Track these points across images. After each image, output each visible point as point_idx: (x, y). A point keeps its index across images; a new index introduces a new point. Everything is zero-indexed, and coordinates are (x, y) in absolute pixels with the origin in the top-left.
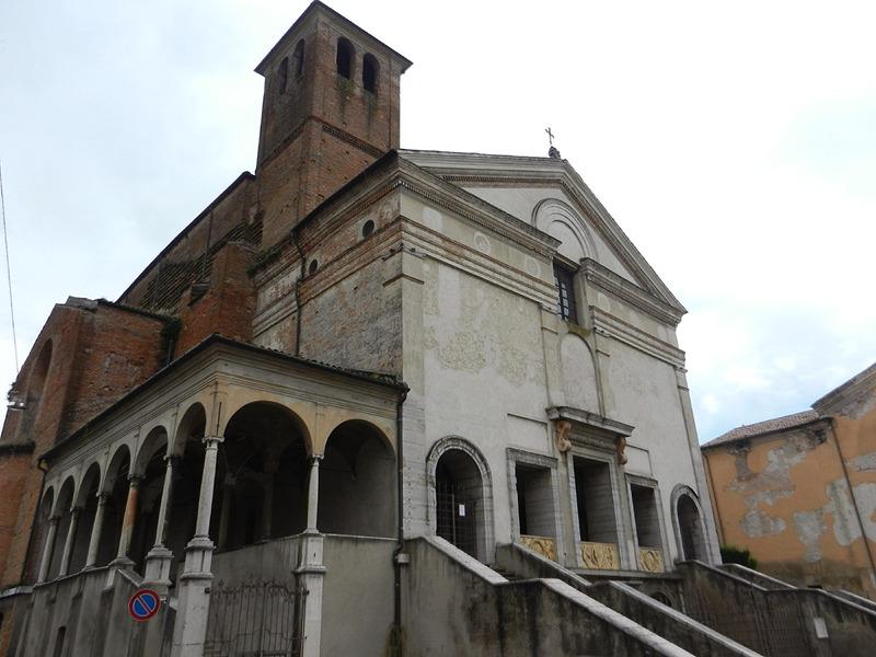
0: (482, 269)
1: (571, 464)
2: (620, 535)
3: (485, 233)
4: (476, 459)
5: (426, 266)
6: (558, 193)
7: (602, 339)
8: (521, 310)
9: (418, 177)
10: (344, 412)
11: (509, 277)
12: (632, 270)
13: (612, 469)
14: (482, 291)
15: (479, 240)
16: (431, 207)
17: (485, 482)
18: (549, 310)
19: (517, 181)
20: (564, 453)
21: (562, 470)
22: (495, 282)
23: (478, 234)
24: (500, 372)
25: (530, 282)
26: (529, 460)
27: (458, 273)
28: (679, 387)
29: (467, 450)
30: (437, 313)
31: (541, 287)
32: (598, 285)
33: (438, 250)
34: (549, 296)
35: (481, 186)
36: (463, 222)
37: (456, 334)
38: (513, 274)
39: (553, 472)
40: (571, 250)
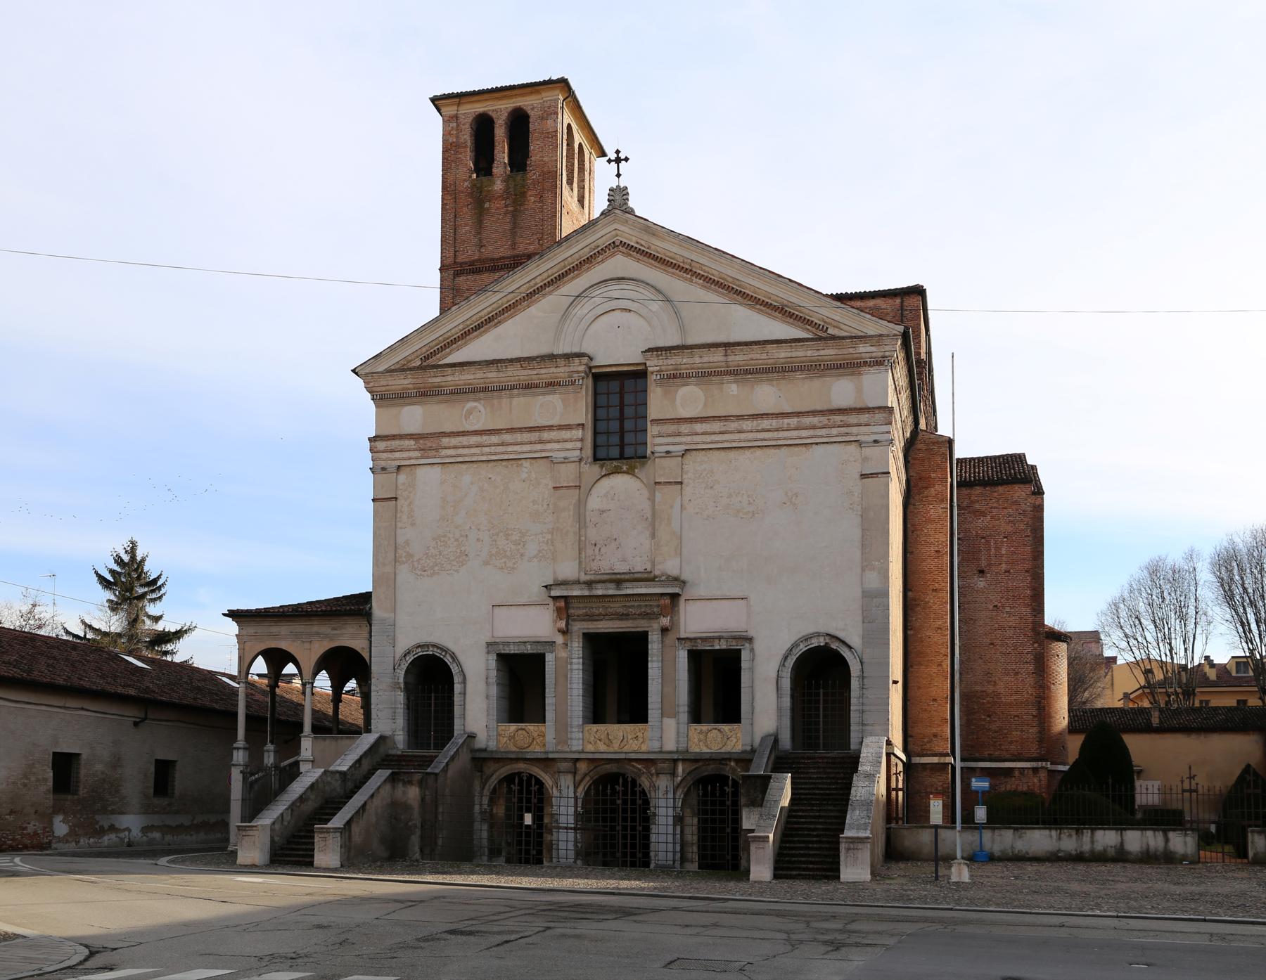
0: (466, 451)
1: (577, 646)
3: (475, 400)
4: (448, 660)
5: (402, 478)
6: (619, 264)
8: (524, 476)
9: (385, 383)
11: (502, 444)
12: (775, 309)
14: (467, 477)
15: (470, 412)
16: (409, 404)
17: (456, 679)
18: (566, 461)
19: (530, 295)
20: (564, 632)
21: (563, 654)
22: (484, 458)
23: (470, 405)
24: (486, 563)
25: (534, 436)
26: (513, 650)
27: (438, 469)
28: (864, 476)
29: (438, 653)
30: (413, 524)
31: (553, 435)
32: (676, 377)
33: (412, 454)
35: (477, 337)
36: (447, 401)
37: (434, 539)
38: (508, 438)
39: (549, 658)
40: (616, 346)
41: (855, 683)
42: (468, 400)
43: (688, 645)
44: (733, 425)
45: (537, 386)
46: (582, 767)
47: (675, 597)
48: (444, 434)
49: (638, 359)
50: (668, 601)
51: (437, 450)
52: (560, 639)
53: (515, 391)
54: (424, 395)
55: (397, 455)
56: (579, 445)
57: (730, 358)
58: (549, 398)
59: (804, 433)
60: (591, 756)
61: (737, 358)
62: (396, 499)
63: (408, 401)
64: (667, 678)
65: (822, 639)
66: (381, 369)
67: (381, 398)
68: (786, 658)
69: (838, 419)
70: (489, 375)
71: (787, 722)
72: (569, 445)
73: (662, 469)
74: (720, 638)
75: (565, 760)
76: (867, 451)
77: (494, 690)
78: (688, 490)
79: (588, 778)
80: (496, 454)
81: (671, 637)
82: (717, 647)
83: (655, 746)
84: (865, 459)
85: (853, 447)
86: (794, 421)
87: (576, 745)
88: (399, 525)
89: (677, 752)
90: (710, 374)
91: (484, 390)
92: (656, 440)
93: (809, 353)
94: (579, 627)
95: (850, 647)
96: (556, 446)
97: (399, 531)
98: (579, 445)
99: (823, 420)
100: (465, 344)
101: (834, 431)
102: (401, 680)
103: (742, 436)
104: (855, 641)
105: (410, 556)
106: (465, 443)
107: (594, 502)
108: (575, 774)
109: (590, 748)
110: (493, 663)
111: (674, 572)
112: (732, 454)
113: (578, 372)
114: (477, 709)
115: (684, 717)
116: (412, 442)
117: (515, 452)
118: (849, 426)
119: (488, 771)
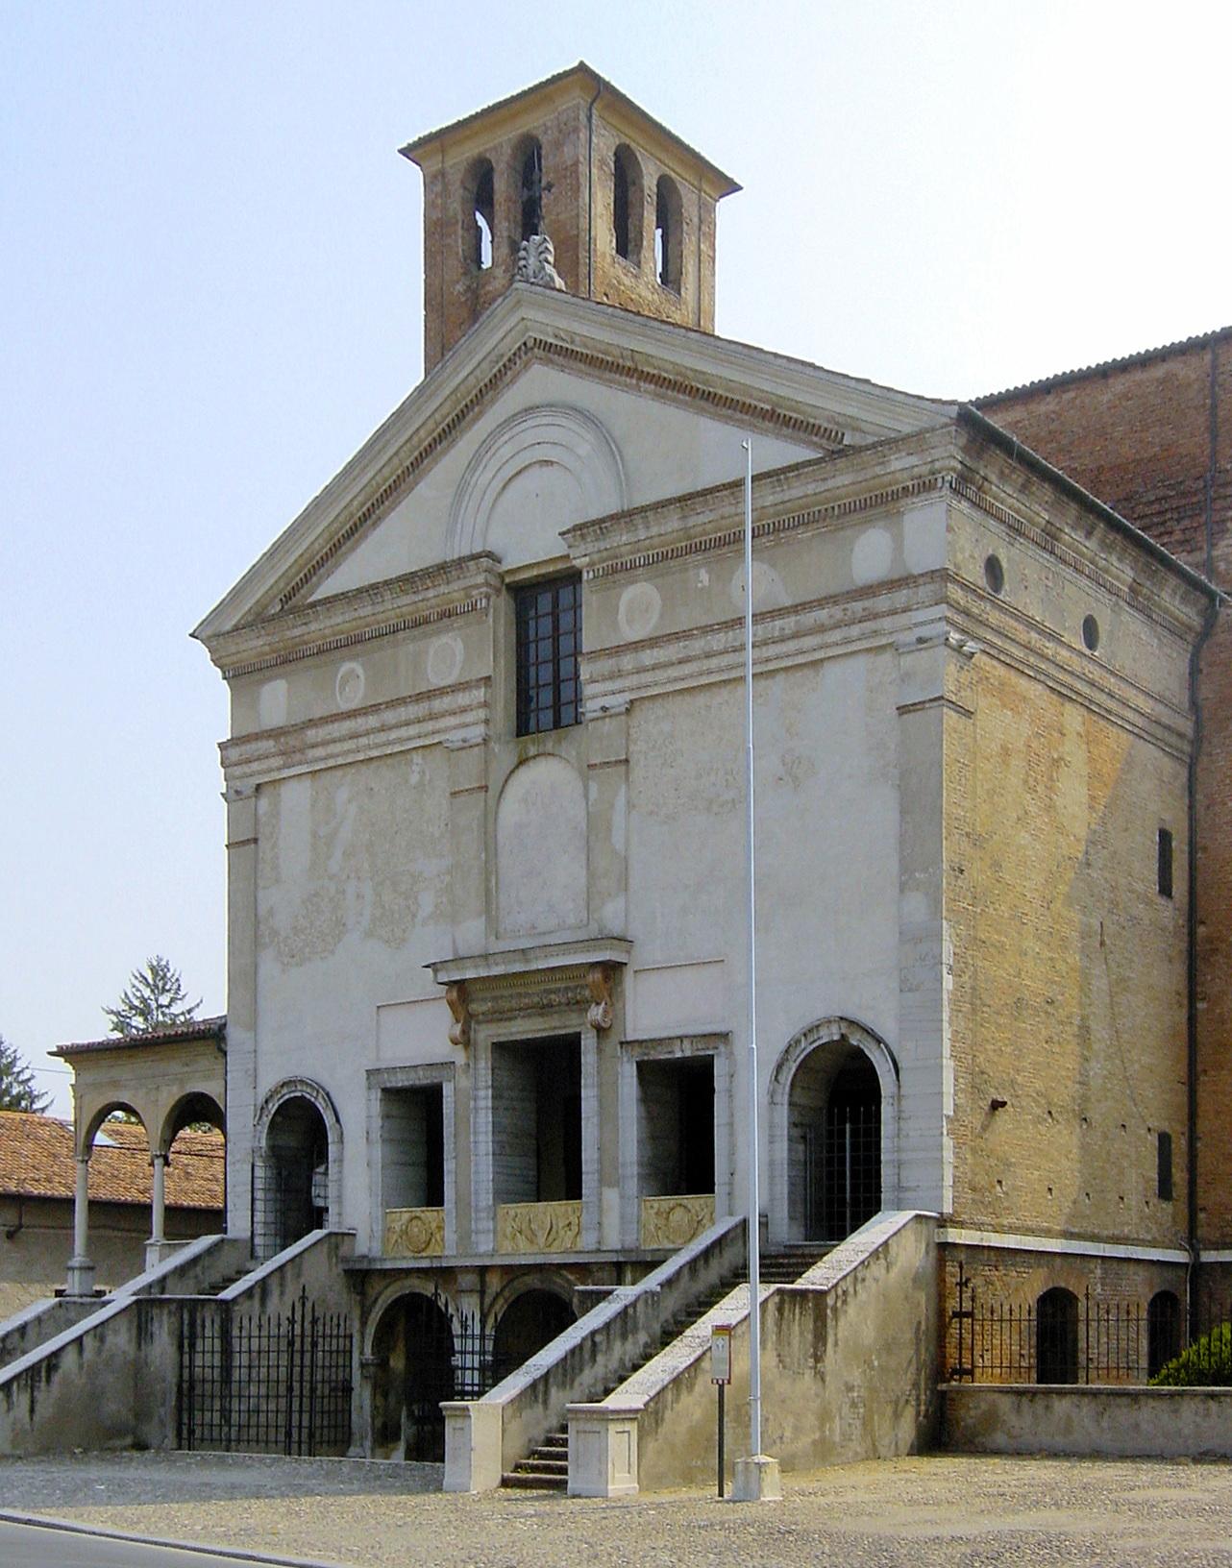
2: (589, 1181)
5: (264, 803)
7: (608, 726)
10: (175, 1089)
11: (383, 729)
13: (588, 1042)
14: (344, 791)
18: (466, 746)
21: (464, 1082)
26: (401, 1081)
27: (307, 782)
28: (903, 710)
30: (277, 881)
32: (618, 571)
34: (464, 710)
35: (353, 549)
39: (448, 1090)
41: (887, 1111)
42: (343, 659)
43: (637, 1054)
44: (697, 646)
45: (427, 621)
46: (494, 1283)
47: (612, 970)
48: (311, 723)
49: (559, 548)
50: (597, 976)
51: (302, 751)
52: (460, 1056)
53: (401, 635)
54: (286, 661)
55: (255, 766)
56: (482, 714)
57: (691, 522)
58: (445, 639)
59: (808, 642)
60: (507, 1261)
61: (701, 519)
62: (256, 840)
63: (267, 673)
64: (614, 1120)
65: (834, 1028)
66: (228, 627)
67: (240, 675)
68: (779, 1067)
69: (858, 606)
70: (362, 613)
71: (783, 1188)
72: (469, 718)
73: (595, 739)
74: (681, 1038)
75: (466, 1269)
76: (907, 661)
77: (378, 1152)
78: (637, 772)
79: (501, 1301)
80: (378, 746)
81: (611, 1045)
82: (679, 1055)
83: (587, 1241)
84: (905, 678)
85: (887, 657)
86: (790, 623)
87: (485, 1244)
88: (261, 883)
89: (623, 1251)
90: (665, 557)
91: (358, 640)
92: (598, 693)
93: (811, 489)
94: (487, 1034)
95: (879, 1041)
96: (452, 721)
97: (261, 894)
98: (482, 714)
99: (837, 612)
100: (337, 565)
101: (855, 631)
102: (264, 1143)
103: (714, 663)
104: (887, 1029)
105: (275, 933)
106: (336, 735)
107: (511, 811)
108: (482, 1293)
109: (507, 1246)
110: (376, 1107)
111: (615, 927)
112: (701, 699)
113: (477, 586)
114: (358, 1184)
115: (632, 1186)
116: (271, 743)
117: (400, 741)
118: (876, 616)
119: (372, 1293)
